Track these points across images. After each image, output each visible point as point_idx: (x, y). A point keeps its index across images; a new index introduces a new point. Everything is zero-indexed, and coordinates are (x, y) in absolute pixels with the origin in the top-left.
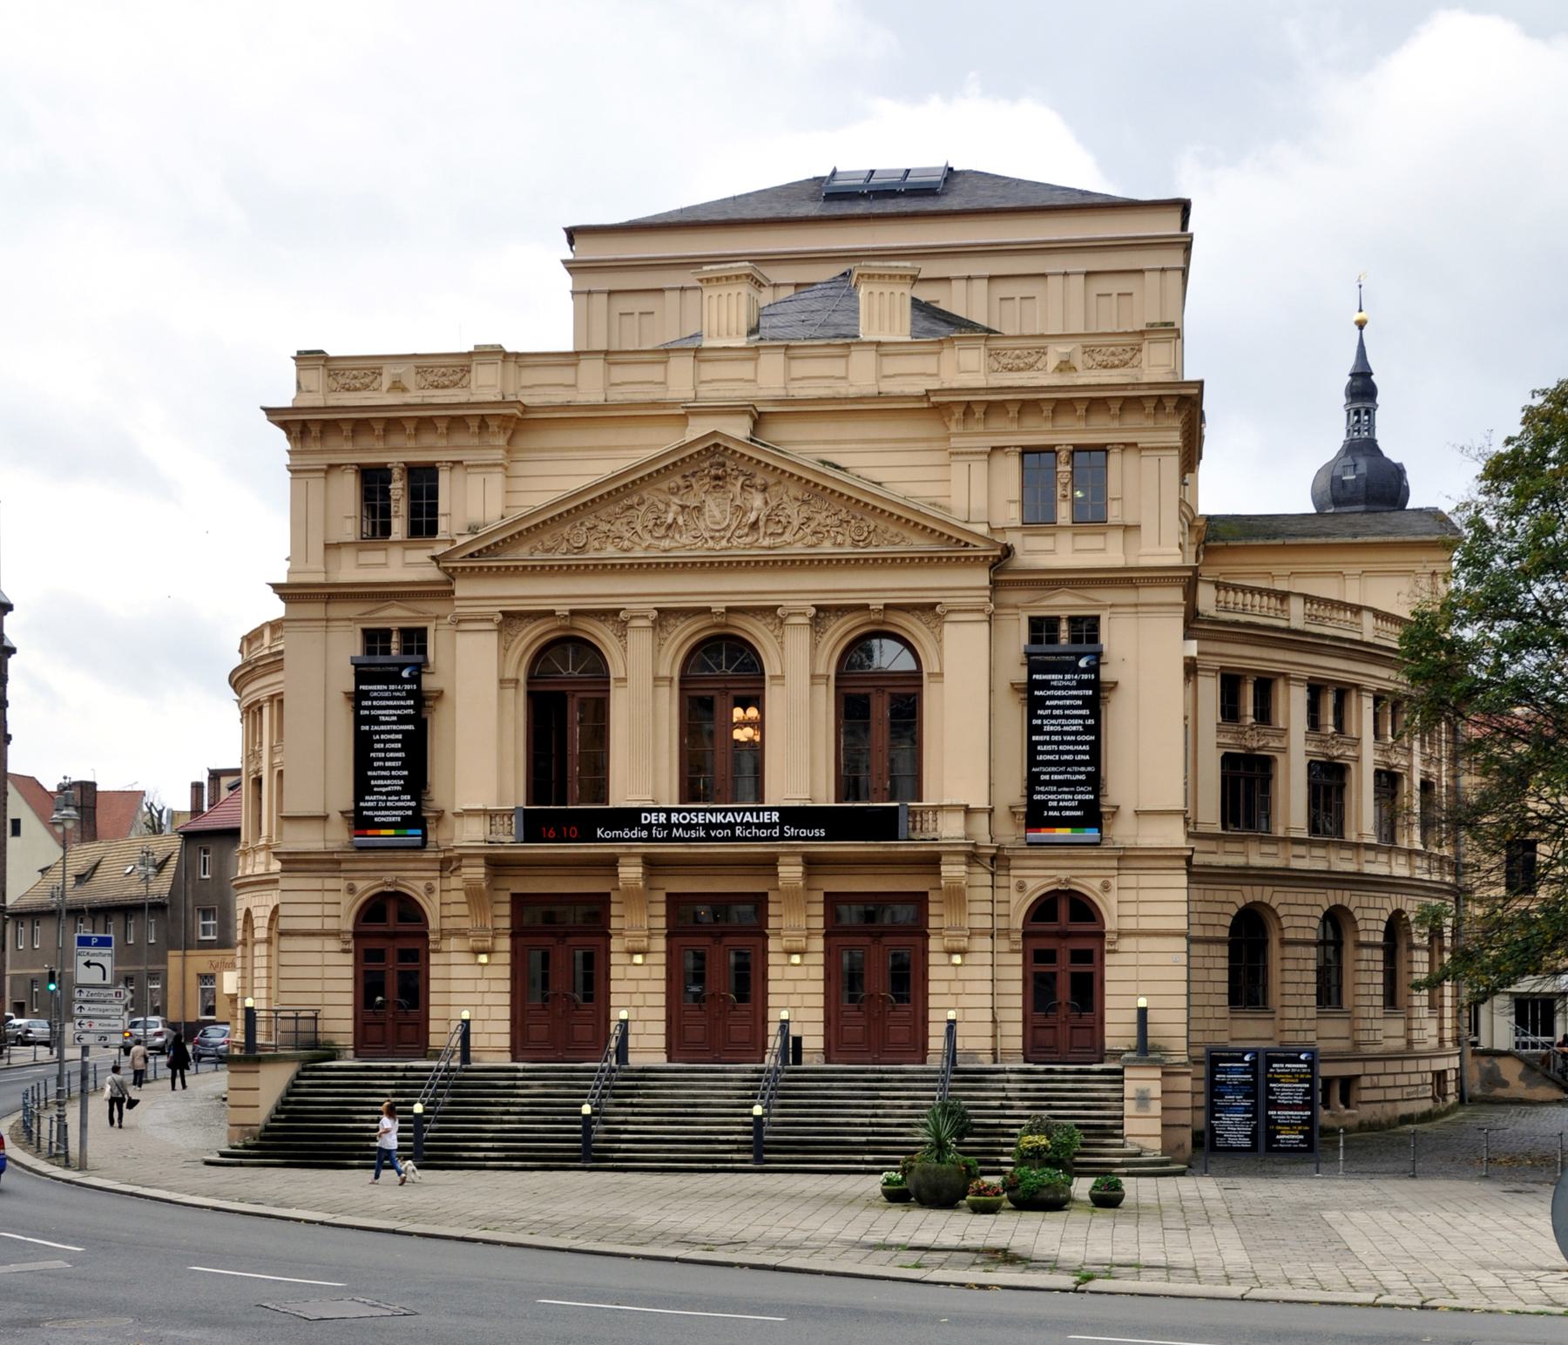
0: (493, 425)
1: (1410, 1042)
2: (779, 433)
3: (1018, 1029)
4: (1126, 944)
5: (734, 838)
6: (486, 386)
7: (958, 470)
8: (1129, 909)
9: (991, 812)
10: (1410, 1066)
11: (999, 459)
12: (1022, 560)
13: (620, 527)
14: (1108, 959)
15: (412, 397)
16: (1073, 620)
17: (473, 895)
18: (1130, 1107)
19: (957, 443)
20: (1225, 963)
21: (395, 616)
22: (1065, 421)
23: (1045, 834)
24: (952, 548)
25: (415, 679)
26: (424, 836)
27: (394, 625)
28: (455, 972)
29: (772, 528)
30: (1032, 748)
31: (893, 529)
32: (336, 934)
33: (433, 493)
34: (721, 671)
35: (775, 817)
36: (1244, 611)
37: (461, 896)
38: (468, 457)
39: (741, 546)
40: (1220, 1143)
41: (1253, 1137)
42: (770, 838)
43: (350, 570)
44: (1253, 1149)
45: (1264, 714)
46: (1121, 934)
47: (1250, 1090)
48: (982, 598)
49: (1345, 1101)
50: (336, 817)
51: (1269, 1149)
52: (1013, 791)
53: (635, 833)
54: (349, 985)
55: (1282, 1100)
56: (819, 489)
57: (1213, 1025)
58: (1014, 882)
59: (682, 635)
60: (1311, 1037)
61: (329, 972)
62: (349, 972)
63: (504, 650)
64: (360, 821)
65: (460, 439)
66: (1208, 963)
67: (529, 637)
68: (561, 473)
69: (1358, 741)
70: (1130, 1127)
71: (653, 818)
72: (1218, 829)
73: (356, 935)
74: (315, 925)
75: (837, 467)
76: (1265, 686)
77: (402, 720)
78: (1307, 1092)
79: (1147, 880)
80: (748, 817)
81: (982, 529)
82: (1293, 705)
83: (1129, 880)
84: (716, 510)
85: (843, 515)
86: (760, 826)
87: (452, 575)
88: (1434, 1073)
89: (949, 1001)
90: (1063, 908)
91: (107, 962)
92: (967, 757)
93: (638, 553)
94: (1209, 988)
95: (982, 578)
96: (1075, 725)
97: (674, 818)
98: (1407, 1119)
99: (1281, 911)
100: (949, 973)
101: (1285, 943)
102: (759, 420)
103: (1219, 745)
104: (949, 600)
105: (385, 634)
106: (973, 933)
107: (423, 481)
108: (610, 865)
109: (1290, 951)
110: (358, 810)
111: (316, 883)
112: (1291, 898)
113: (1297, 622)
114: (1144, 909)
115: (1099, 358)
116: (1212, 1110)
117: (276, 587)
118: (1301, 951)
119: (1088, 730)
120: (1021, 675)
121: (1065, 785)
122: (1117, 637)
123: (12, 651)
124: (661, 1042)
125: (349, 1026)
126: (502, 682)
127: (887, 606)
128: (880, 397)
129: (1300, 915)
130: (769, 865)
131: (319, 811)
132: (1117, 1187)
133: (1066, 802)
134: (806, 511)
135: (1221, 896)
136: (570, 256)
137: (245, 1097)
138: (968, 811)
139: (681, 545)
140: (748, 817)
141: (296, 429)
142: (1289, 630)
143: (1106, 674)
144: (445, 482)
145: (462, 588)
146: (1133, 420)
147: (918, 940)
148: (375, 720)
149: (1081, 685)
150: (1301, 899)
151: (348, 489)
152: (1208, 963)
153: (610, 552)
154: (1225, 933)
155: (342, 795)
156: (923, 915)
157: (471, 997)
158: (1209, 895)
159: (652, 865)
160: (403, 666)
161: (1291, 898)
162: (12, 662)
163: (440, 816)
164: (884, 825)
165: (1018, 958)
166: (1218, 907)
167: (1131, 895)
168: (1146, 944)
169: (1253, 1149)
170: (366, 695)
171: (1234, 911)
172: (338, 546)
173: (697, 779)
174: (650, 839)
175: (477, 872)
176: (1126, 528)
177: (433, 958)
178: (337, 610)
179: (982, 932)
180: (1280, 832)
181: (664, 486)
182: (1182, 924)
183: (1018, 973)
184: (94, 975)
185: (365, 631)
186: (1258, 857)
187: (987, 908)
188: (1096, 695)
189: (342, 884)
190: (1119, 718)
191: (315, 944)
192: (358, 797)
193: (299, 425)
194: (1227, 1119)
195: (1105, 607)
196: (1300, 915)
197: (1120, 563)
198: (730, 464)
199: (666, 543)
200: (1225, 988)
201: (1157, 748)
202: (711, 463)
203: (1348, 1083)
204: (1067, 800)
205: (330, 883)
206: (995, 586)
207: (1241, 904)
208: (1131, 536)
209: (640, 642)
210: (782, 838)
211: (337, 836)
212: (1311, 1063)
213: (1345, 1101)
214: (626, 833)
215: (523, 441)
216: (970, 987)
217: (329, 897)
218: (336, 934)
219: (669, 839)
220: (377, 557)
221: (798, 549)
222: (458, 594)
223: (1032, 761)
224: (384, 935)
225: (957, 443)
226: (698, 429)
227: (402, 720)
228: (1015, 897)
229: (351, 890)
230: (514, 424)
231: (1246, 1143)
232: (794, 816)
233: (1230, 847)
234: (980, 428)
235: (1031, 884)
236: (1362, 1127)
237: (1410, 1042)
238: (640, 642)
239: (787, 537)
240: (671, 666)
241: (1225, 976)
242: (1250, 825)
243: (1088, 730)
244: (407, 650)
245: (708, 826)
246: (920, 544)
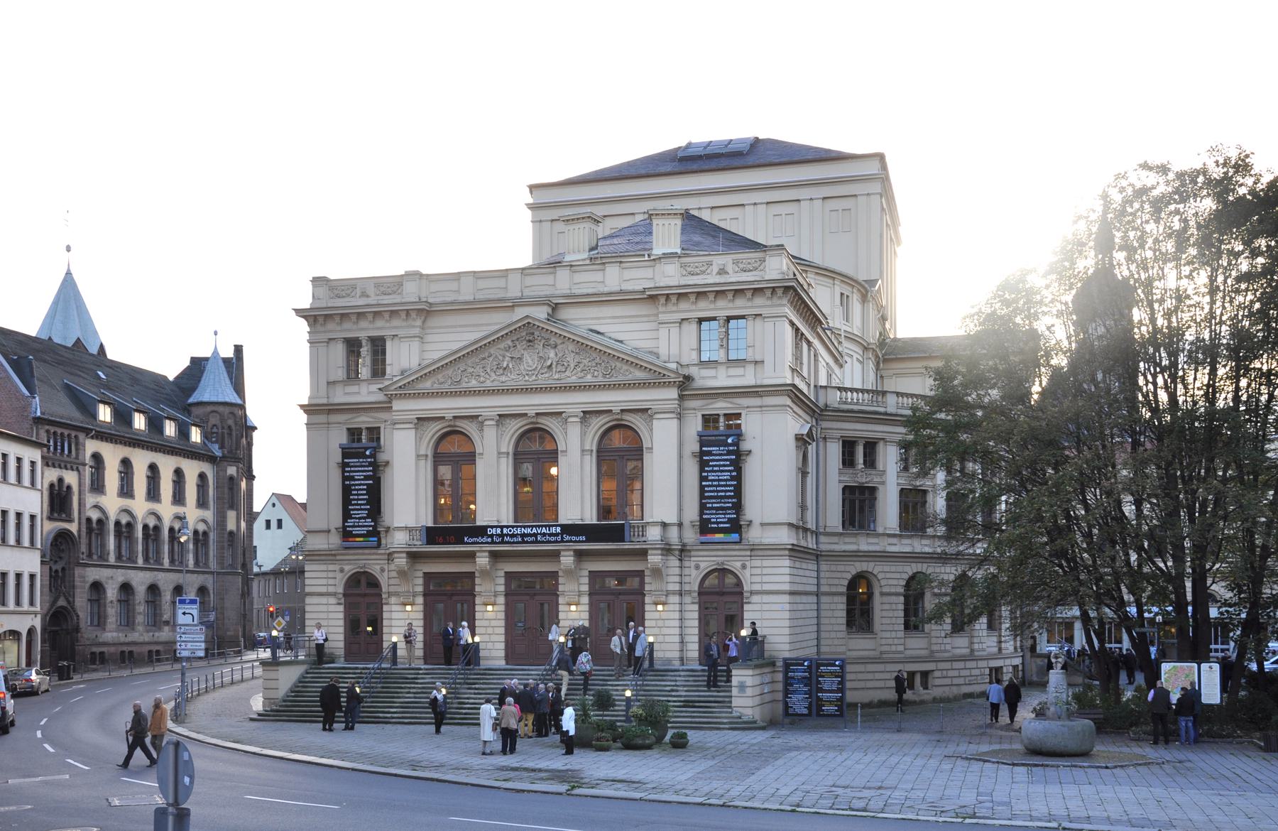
0: (413, 315)
1: (972, 651)
2: (565, 314)
3: (696, 646)
4: (755, 598)
5: (537, 542)
6: (411, 293)
7: (663, 332)
8: (758, 579)
9: (680, 525)
10: (969, 664)
11: (685, 326)
12: (699, 383)
13: (479, 370)
14: (746, 607)
15: (372, 300)
16: (728, 417)
17: (402, 574)
18: (735, 691)
19: (662, 317)
20: (844, 606)
21: (363, 421)
22: (721, 303)
23: (709, 537)
24: (657, 379)
25: (373, 456)
26: (379, 540)
27: (363, 426)
28: (395, 615)
29: (560, 368)
30: (702, 489)
31: (625, 367)
32: (334, 594)
33: (384, 353)
34: (535, 448)
35: (559, 530)
36: (857, 403)
37: (394, 574)
38: (400, 333)
39: (544, 379)
40: (791, 711)
41: (809, 708)
42: (556, 542)
43: (340, 396)
44: (809, 715)
45: (870, 462)
46: (752, 593)
47: (807, 681)
48: (674, 405)
49: (925, 685)
50: (333, 530)
51: (818, 715)
52: (692, 513)
53: (485, 540)
54: (342, 623)
55: (826, 687)
56: (583, 347)
57: (836, 642)
58: (693, 564)
59: (514, 428)
60: (901, 648)
61: (331, 616)
62: (341, 616)
63: (418, 440)
64: (346, 534)
65: (396, 322)
66: (833, 606)
67: (434, 430)
68: (447, 339)
70: (735, 702)
71: (494, 531)
72: (840, 530)
73: (345, 595)
74: (323, 589)
75: (598, 333)
76: (871, 447)
77: (366, 478)
78: (840, 683)
79: (766, 563)
80: (544, 530)
81: (673, 366)
82: (889, 458)
83: (757, 563)
84: (530, 360)
85: (598, 360)
86: (550, 535)
87: (390, 399)
88: (991, 669)
89: (656, 631)
91: (195, 612)
92: (666, 493)
93: (488, 383)
94: (833, 621)
95: (673, 393)
96: (726, 476)
97: (505, 531)
98: (971, 695)
99: (880, 576)
100: (656, 615)
101: (882, 594)
102: (555, 307)
103: (840, 481)
104: (655, 407)
105: (359, 431)
106: (668, 593)
107: (378, 346)
108: (471, 556)
109: (886, 599)
110: (344, 527)
111: (323, 567)
112: (887, 569)
113: (891, 409)
114: (765, 579)
115: (741, 266)
116: (787, 693)
117: (302, 406)
118: (893, 599)
119: (732, 478)
120: (696, 448)
121: (722, 511)
122: (751, 424)
123: (255, 428)
124: (502, 654)
125: (342, 645)
126: (418, 456)
127: (622, 411)
128: (621, 292)
129: (891, 579)
130: (555, 555)
131: (325, 527)
132: (684, 736)
133: (721, 519)
134: (577, 359)
135: (841, 568)
136: (531, 201)
137: (272, 684)
138: (664, 525)
139: (510, 380)
140: (544, 530)
141: (311, 320)
142: (886, 414)
143: (745, 446)
144: (389, 346)
145: (397, 405)
146: (759, 301)
147: (640, 597)
148: (352, 478)
149: (729, 453)
150: (893, 569)
151: (339, 351)
152: (833, 606)
153: (474, 383)
154: (844, 589)
155: (337, 521)
156: (642, 583)
158: (833, 568)
159: (495, 556)
160: (366, 449)
161: (887, 569)
162: (255, 434)
163: (388, 530)
164: (616, 533)
165: (696, 607)
166: (839, 575)
167: (758, 571)
168: (766, 598)
169: (809, 715)
170: (347, 465)
171: (849, 576)
172: (334, 383)
173: (520, 509)
174: (493, 542)
175: (401, 561)
176: (756, 362)
177: (385, 608)
179: (674, 593)
180: (880, 530)
181: (502, 346)
182: (787, 587)
183: (696, 615)
184: (188, 620)
185: (348, 429)
186: (864, 544)
187: (677, 579)
188: (738, 459)
189: (337, 567)
190: (753, 472)
191: (324, 600)
192: (345, 520)
193: (312, 317)
194: (795, 698)
195: (744, 408)
196: (891, 579)
197: (752, 383)
198: (537, 333)
199: (503, 378)
200: (844, 621)
201: (771, 491)
202: (527, 333)
203: (925, 675)
204: (722, 518)
205: (331, 567)
206: (682, 398)
207: (854, 572)
208: (759, 366)
209: (490, 433)
210: (562, 541)
211: (335, 540)
212: (842, 667)
213: (926, 688)
214: (480, 540)
215: (434, 322)
216: (668, 623)
217: (331, 575)
218: (334, 594)
219: (502, 542)
220: (354, 389)
221: (574, 379)
222: (394, 408)
223: (702, 496)
224: (359, 595)
225: (662, 317)
226: (520, 313)
227: (366, 478)
228: (694, 572)
229: (342, 571)
230: (426, 312)
231: (805, 711)
232: (570, 529)
233: (847, 540)
234: (674, 308)
235: (702, 565)
236: (935, 700)
237: (1000, 649)
238: (490, 433)
239: (568, 373)
240: (508, 445)
241: (844, 613)
242: (861, 527)
243: (732, 478)
244: (371, 440)
245: (523, 535)
246: (640, 375)
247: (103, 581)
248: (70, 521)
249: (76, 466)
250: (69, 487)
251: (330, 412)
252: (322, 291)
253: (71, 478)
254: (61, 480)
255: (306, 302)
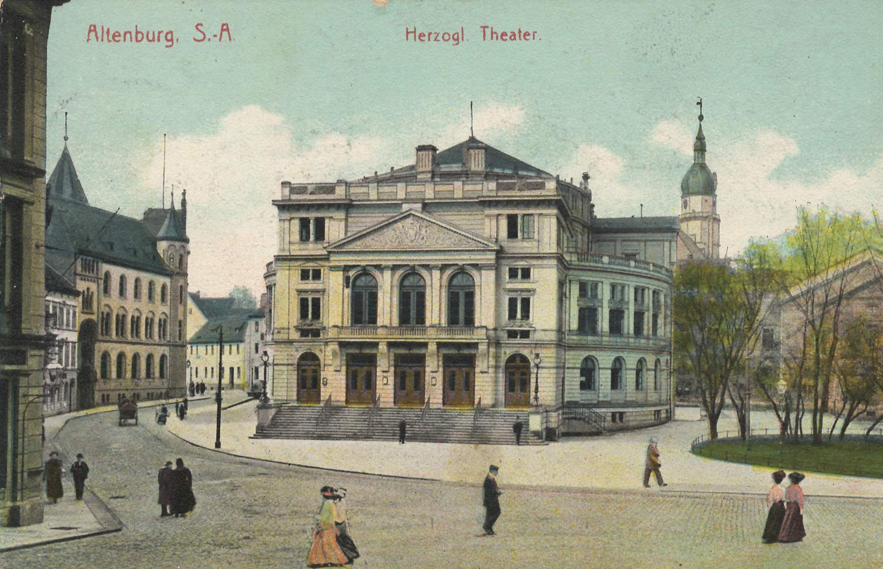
16: (523, 269)
17: (334, 354)
43: (297, 250)
69: (628, 303)
90: (518, 359)
95: (492, 256)
107: (320, 224)
151: (296, 225)
157: (334, 383)
178: (293, 263)
215: (351, 210)
230: (348, 207)
247: (109, 350)
248: (92, 314)
249: (96, 280)
250: (92, 293)
251: (290, 260)
252: (287, 191)
253: (93, 287)
254: (88, 289)
255: (278, 197)
